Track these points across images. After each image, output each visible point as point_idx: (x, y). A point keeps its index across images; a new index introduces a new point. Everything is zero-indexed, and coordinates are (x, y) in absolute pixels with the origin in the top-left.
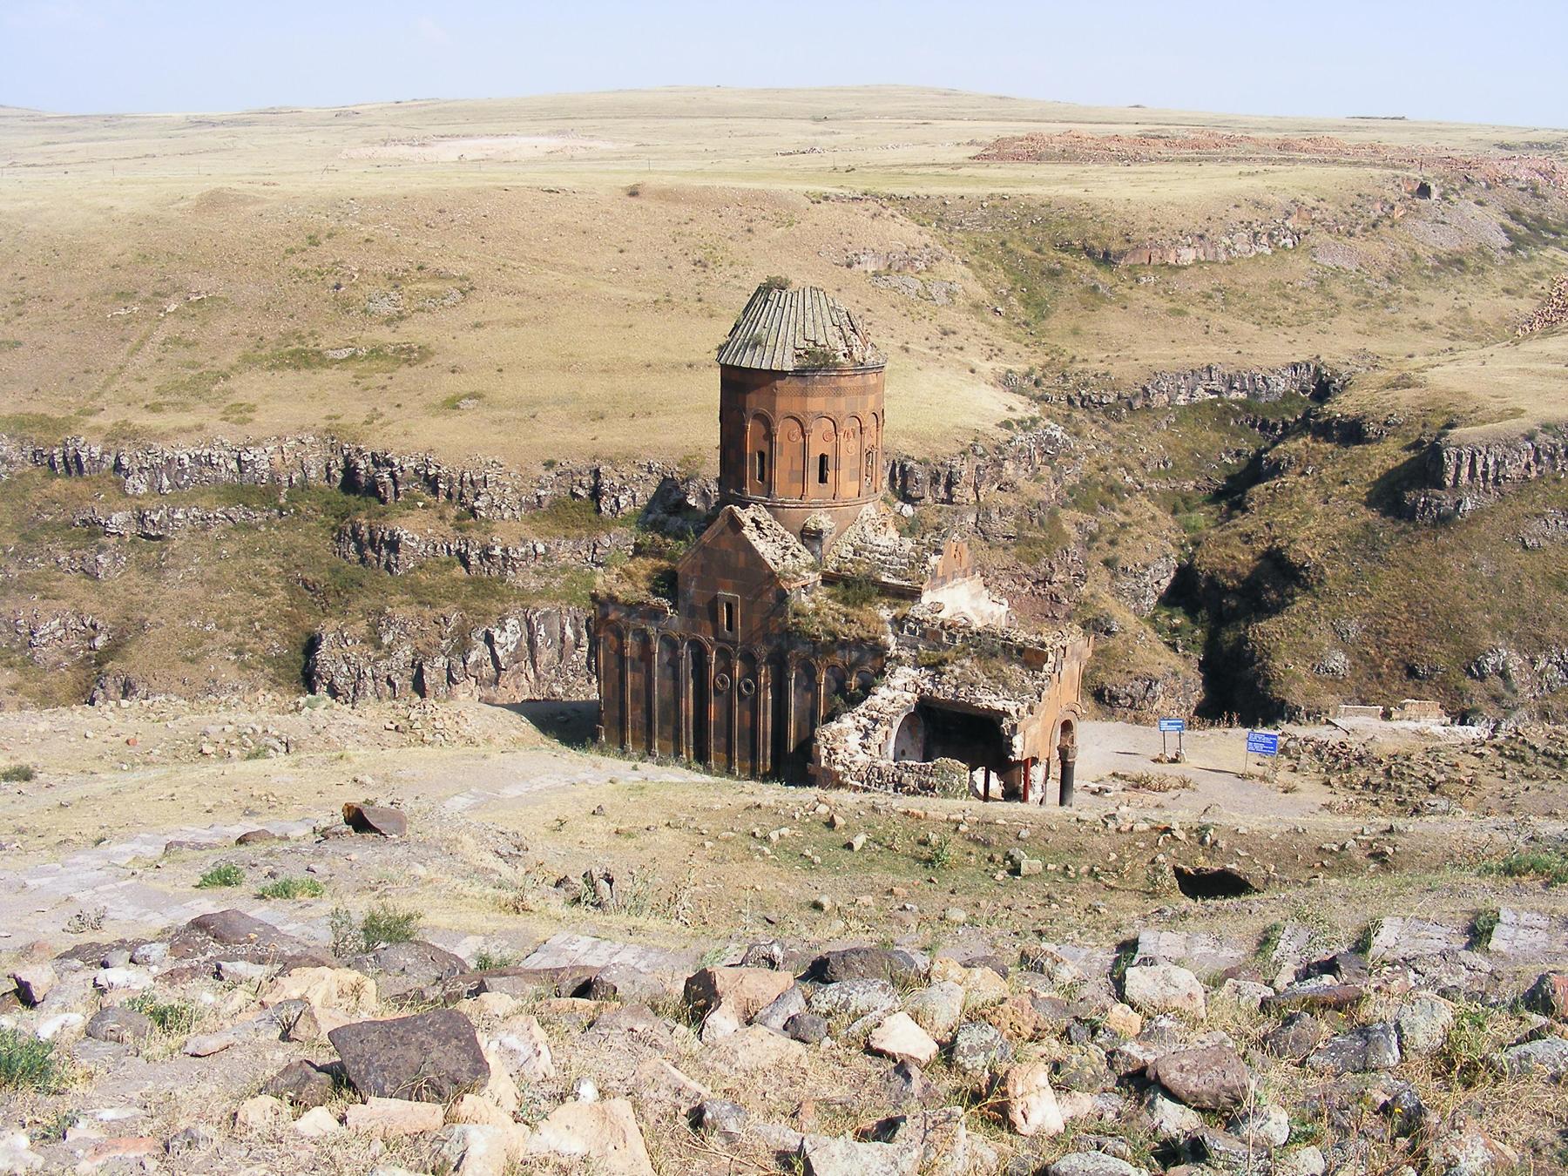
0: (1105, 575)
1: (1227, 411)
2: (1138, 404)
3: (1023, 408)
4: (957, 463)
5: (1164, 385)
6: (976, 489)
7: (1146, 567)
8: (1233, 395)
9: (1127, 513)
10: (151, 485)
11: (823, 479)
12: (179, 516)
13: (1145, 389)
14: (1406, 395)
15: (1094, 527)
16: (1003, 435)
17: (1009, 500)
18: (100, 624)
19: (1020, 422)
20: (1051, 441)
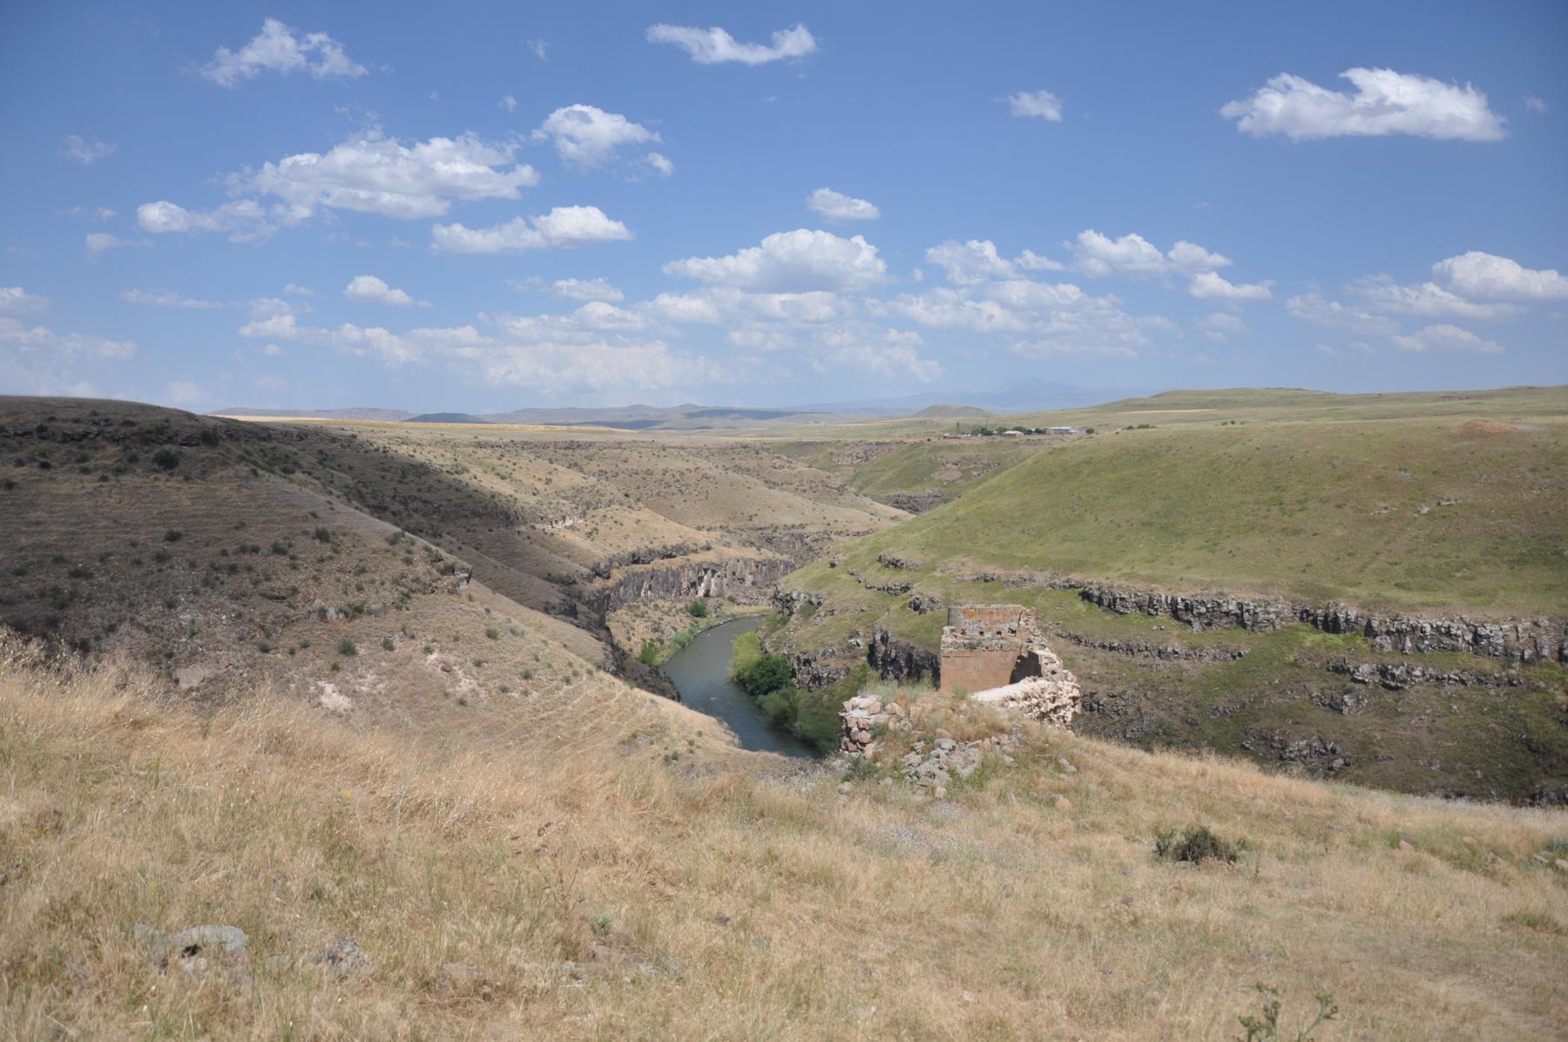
10: (1395, 647)
12: (1417, 673)
18: (1339, 749)
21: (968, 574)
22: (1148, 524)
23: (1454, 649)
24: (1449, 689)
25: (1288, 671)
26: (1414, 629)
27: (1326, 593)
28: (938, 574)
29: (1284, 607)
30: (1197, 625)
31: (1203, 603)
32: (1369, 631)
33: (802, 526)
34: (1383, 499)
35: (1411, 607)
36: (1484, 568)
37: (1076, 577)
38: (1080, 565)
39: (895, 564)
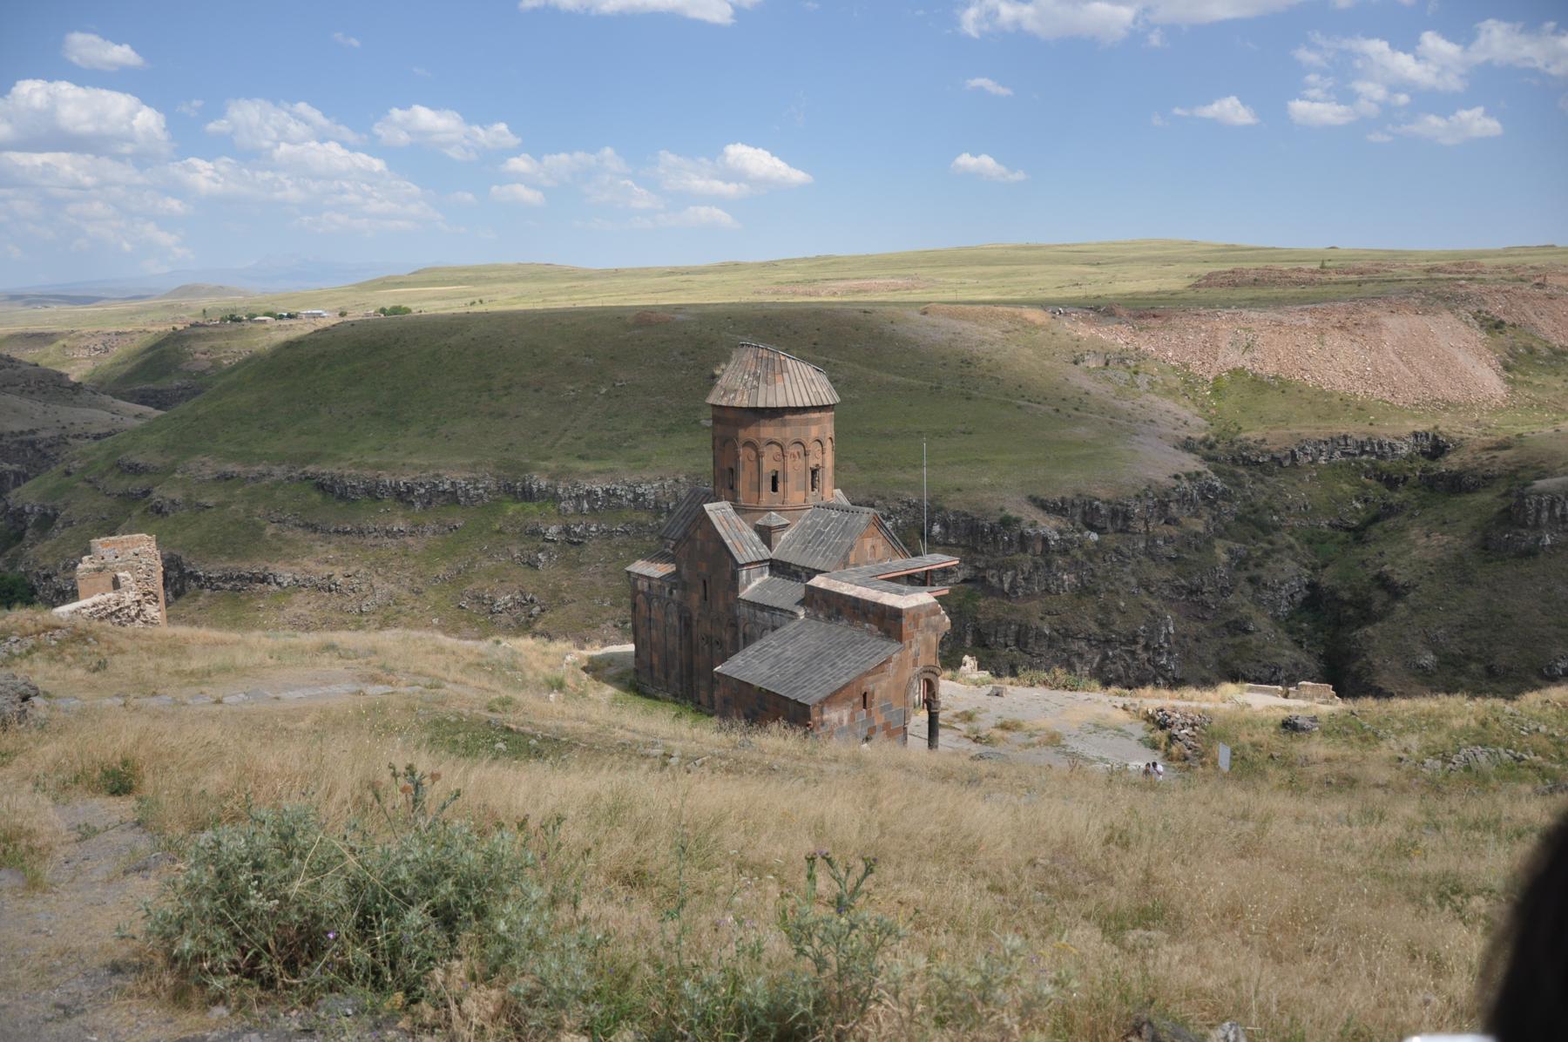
0: (1249, 590)
1: (1359, 469)
2: (1287, 463)
3: (1191, 463)
4: (1132, 503)
5: (1309, 449)
6: (1147, 523)
7: (1282, 583)
8: (1365, 457)
9: (1271, 543)
10: (576, 508)
11: (775, 489)
13: (1293, 452)
14: (1502, 454)
15: (1243, 553)
16: (1174, 483)
17: (1173, 531)
19: (1188, 475)
20: (1212, 489)
21: (208, 473)
22: (378, 414)
23: (620, 507)
24: (617, 540)
25: (495, 538)
26: (589, 493)
27: (526, 469)
28: (177, 476)
29: (490, 482)
30: (418, 505)
31: (421, 485)
32: (556, 498)
33: (32, 432)
34: (571, 383)
35: (587, 475)
36: (644, 438)
37: (311, 469)
38: (314, 457)
39: (135, 470)
